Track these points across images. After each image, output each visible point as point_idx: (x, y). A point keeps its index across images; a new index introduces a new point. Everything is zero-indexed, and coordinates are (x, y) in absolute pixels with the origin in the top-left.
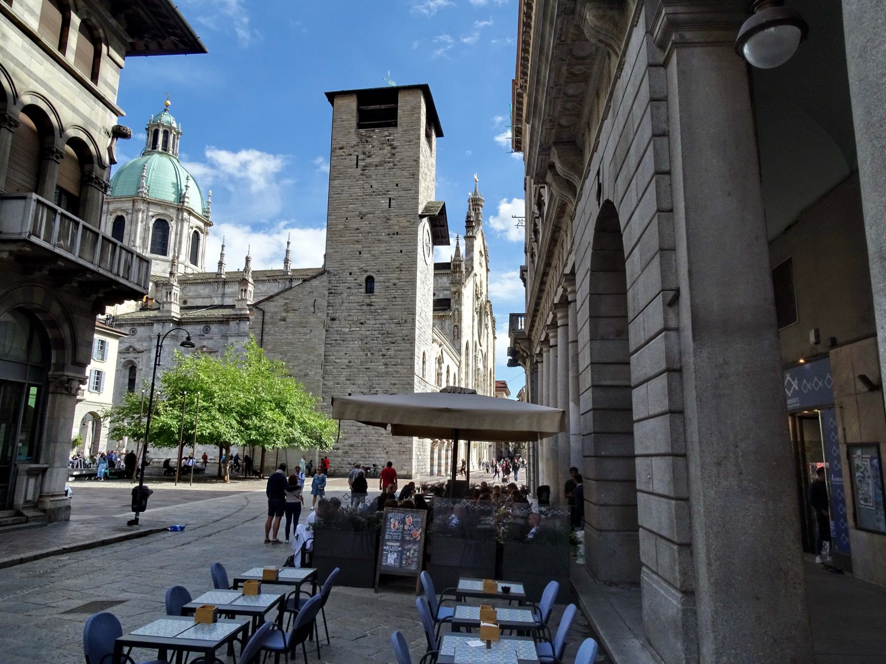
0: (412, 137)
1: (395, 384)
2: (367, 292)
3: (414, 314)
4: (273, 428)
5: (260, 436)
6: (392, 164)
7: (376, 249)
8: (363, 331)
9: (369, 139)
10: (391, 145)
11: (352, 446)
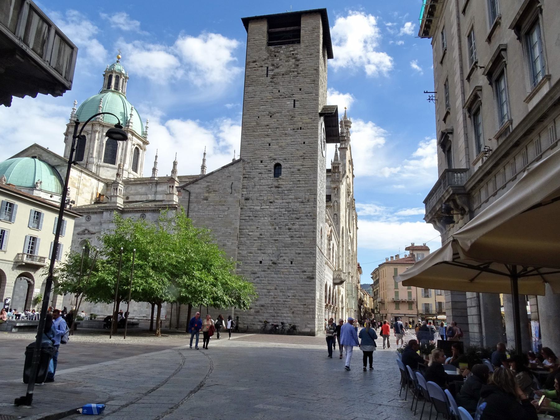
0: (313, 51)
1: (299, 254)
2: (275, 176)
3: (316, 194)
4: (201, 286)
5: (189, 293)
6: (296, 73)
7: (283, 141)
8: (272, 208)
9: (277, 54)
10: (295, 58)
11: (262, 306)
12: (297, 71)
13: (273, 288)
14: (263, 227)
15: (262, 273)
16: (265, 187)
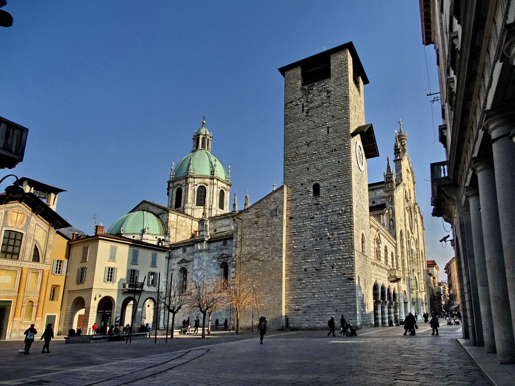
6: (328, 104)
10: (327, 90)
11: (309, 307)
14: (306, 240)
15: (307, 279)
16: (306, 205)
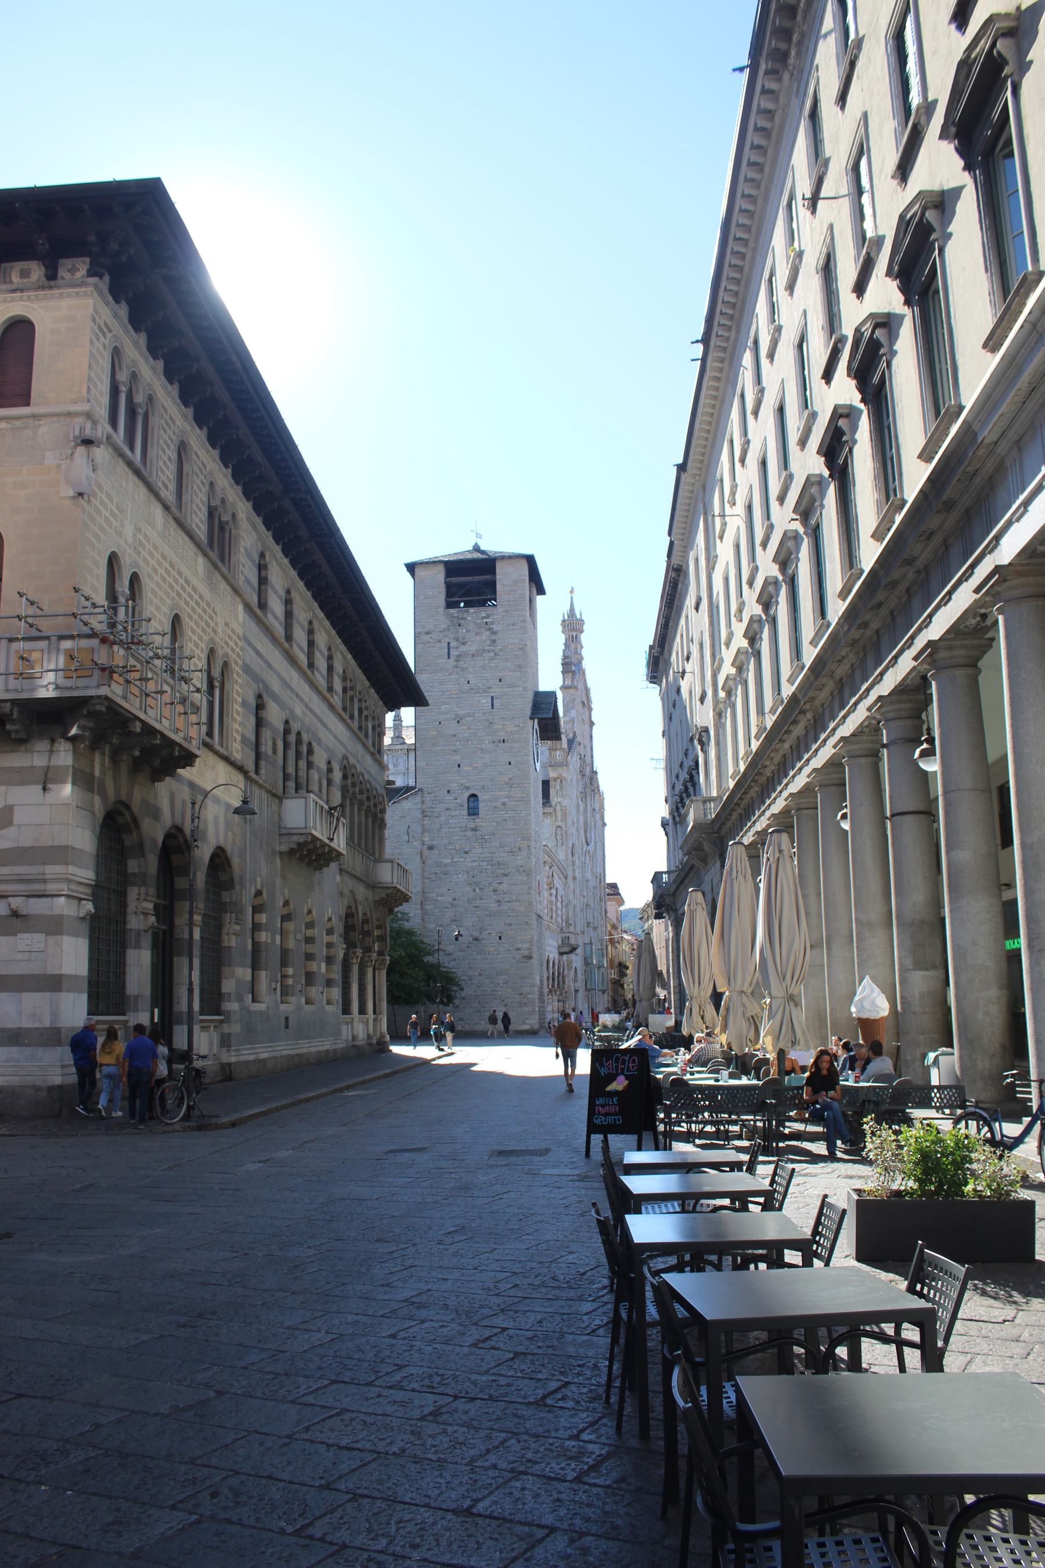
1: (511, 925)
2: (469, 815)
6: (492, 654)
9: (462, 622)
10: (490, 629)
12: (493, 650)
13: (476, 973)
